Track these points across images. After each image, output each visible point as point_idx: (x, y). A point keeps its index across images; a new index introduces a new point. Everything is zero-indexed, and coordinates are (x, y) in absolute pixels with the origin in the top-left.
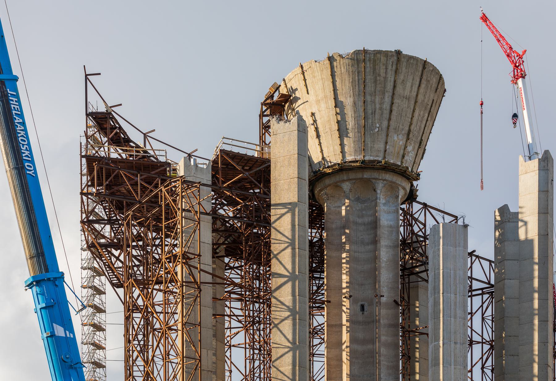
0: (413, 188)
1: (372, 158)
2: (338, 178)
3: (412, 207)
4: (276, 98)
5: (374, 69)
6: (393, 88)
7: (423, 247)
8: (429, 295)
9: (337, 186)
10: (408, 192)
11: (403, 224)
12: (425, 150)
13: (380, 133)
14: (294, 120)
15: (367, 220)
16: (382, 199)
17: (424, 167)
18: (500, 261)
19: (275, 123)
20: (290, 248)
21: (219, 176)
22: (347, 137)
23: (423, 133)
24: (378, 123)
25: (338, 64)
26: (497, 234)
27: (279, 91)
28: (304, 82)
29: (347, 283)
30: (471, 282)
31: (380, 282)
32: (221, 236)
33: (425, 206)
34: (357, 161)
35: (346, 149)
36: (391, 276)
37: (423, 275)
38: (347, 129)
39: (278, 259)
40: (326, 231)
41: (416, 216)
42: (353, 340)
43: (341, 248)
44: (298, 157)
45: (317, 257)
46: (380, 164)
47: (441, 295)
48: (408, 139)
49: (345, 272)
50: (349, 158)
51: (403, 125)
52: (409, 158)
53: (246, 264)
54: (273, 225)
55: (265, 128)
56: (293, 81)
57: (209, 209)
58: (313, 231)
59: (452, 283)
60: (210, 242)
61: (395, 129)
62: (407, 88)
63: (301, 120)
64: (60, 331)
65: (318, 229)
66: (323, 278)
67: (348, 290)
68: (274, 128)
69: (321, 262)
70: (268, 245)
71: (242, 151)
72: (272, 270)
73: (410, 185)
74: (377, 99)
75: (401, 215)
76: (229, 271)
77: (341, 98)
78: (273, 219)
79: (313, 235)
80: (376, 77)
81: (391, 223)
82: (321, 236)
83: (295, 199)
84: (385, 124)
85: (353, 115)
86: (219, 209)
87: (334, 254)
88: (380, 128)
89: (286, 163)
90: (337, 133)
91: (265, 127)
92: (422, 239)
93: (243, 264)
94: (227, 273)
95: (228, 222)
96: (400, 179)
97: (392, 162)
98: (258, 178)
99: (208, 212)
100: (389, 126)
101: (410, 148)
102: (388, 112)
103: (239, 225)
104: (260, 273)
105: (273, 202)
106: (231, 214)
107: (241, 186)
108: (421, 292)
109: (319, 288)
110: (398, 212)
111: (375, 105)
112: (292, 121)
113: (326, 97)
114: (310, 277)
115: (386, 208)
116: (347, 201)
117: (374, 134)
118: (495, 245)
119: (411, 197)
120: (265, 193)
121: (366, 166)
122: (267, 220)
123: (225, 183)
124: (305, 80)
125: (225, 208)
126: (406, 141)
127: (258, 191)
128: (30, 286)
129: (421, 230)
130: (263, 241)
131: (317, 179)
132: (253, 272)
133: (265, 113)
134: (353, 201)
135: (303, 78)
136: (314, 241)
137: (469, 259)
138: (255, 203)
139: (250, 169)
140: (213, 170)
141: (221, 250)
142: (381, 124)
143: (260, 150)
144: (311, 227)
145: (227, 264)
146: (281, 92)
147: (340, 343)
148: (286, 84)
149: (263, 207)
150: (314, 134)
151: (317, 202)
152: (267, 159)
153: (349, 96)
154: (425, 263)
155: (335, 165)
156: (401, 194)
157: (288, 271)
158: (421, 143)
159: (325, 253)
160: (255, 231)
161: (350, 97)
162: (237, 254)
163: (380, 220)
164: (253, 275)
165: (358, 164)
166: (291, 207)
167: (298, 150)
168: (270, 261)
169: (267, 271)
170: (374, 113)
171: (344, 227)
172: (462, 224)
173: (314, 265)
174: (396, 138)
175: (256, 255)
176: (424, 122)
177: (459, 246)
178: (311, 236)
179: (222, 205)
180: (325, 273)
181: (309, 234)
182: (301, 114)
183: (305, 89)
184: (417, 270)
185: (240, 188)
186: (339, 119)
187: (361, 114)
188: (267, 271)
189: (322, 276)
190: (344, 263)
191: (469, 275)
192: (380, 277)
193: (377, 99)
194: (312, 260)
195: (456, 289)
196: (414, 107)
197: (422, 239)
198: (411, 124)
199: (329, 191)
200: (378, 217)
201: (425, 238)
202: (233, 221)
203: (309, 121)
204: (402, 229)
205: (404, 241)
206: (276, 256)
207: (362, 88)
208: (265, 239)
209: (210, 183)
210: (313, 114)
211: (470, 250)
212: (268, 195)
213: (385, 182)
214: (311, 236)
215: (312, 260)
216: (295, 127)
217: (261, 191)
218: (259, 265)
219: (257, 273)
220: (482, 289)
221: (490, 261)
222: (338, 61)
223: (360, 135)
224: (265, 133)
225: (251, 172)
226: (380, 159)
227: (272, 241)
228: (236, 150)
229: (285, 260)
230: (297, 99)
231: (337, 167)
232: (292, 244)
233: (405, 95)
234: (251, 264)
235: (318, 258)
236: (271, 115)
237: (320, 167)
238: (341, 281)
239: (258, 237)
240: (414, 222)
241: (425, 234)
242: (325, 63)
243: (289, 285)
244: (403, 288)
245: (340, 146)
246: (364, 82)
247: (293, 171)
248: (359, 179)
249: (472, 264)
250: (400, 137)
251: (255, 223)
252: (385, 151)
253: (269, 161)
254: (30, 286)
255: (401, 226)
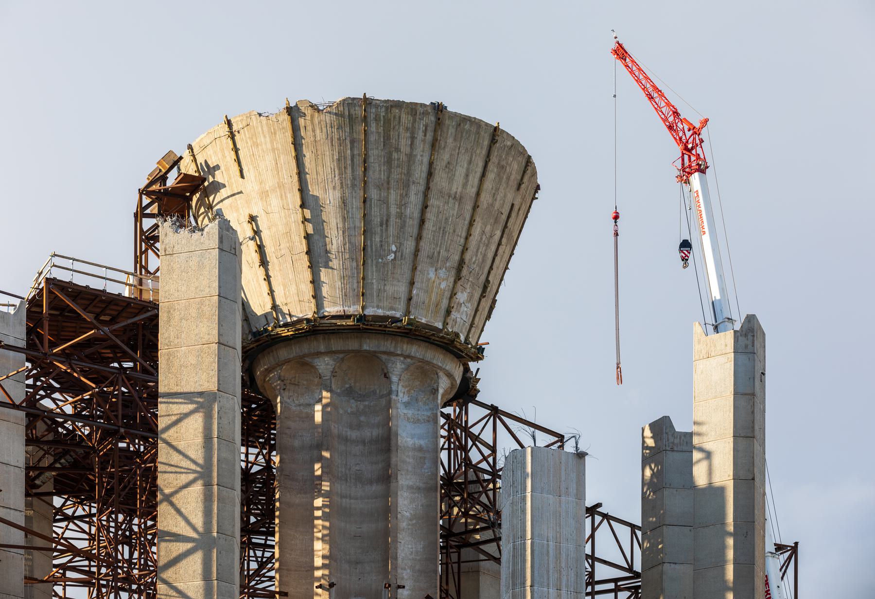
0: (469, 375)
1: (380, 312)
2: (305, 348)
3: (467, 413)
4: (172, 180)
5: (387, 138)
6: (425, 182)
7: (491, 494)
8: (503, 589)
9: (304, 364)
10: (458, 382)
11: (446, 446)
12: (494, 301)
13: (398, 262)
14: (212, 228)
15: (368, 433)
16: (401, 395)
17: (491, 335)
18: (653, 525)
19: (170, 232)
20: (200, 482)
21: (45, 332)
22: (327, 266)
23: (491, 268)
24: (394, 243)
25: (308, 123)
26: (648, 473)
27: (179, 168)
28: (233, 153)
29: (324, 557)
30: (592, 566)
31: (396, 559)
32: (47, 453)
33: (495, 412)
34: (348, 317)
35: (325, 290)
36: (420, 547)
37: (491, 548)
38: (327, 252)
39: (172, 504)
40: (279, 453)
41: (475, 430)
43: (313, 486)
44: (220, 301)
45: (259, 502)
46: (399, 324)
47: (528, 589)
48: (458, 278)
49: (320, 535)
50: (331, 309)
51: (447, 250)
53: (100, 512)
54: (164, 436)
55: (148, 240)
56: (210, 151)
57: (19, 395)
58: (251, 450)
59: (551, 566)
60: (22, 463)
61: (431, 257)
63: (226, 229)
65: (263, 447)
66: (273, 547)
67: (327, 572)
68: (167, 241)
69: (268, 514)
70: (151, 475)
71: (96, 284)
72: (160, 526)
73: (462, 368)
74: (393, 196)
75: (442, 427)
76: (63, 524)
77: (314, 190)
78: (162, 423)
79: (251, 458)
80: (390, 153)
81: (422, 442)
82: (269, 461)
83: (211, 385)
84: (409, 246)
85: (340, 225)
86: (43, 397)
87: (297, 499)
88: (399, 254)
89: (193, 312)
90: (306, 258)
91: (148, 239)
92: (487, 477)
93: (94, 511)
94: (59, 528)
95: (61, 425)
96: (441, 357)
97: (424, 321)
98: (129, 339)
99: (17, 403)
100: (417, 250)
101: (462, 297)
102: (416, 222)
103: (87, 432)
104: (131, 530)
105: (162, 389)
106: (69, 410)
107: (93, 354)
108: (485, 582)
109: (262, 565)
110: (436, 422)
111: (388, 208)
112: (206, 230)
113: (281, 186)
114: (242, 543)
115: (410, 412)
116: (325, 394)
117: (385, 265)
118: (643, 494)
119: (466, 392)
120: (144, 370)
121: (365, 326)
122: (149, 424)
123: (57, 346)
124: (236, 150)
125: (57, 395)
126: (455, 282)
127: (131, 364)
129: (485, 459)
130: (139, 467)
132: (117, 528)
133: (148, 211)
134: (339, 395)
135: (232, 146)
136: (253, 471)
137: (588, 521)
138: (123, 389)
139: (113, 321)
140: (29, 318)
141: (46, 482)
142: (400, 247)
143: (135, 283)
144: (246, 443)
145: (59, 510)
146: (183, 171)
148: (194, 156)
149: (140, 398)
150: (256, 257)
151: (261, 394)
152: (150, 302)
153: (331, 186)
154: (494, 525)
155: (300, 321)
156: (444, 384)
157: (194, 529)
158: (485, 288)
159: (277, 496)
160: (122, 445)
161: (334, 188)
162: (82, 491)
163: (397, 435)
164: (116, 534)
165: (350, 322)
166: (203, 401)
167: (220, 287)
168: (155, 507)
169: (147, 528)
170: (385, 223)
171: (319, 447)
172: (573, 450)
173: (253, 519)
174: (432, 275)
175: (123, 493)
176: (493, 248)
177: (567, 494)
178: (247, 462)
179: (52, 389)
180: (277, 535)
181: (243, 457)
182: (228, 215)
183: (237, 168)
184: (478, 537)
185: (91, 358)
186: (310, 230)
187: (358, 224)
188: (147, 528)
189: (269, 543)
190: (318, 518)
191: (588, 551)
192: (396, 549)
193: (393, 196)
194: (249, 510)
195: (559, 579)
196: (472, 216)
197: (487, 477)
198: (465, 249)
199: (285, 372)
200: (394, 429)
201: (495, 474)
202: (73, 423)
203: (244, 231)
204: (444, 455)
205: (448, 479)
206: (168, 498)
208: (145, 462)
209: (22, 344)
210: (252, 219)
211: (589, 503)
212: (152, 375)
213: (409, 360)
214: (247, 462)
215: (249, 510)
216: (214, 242)
217: (135, 365)
218: (130, 514)
219: (125, 530)
220: (615, 581)
221: (633, 527)
222: (308, 118)
223: (354, 264)
224: (146, 250)
225: (115, 327)
226: (398, 315)
227: (161, 468)
228: (81, 281)
229: (187, 505)
230: (217, 187)
231: (304, 325)
232: (204, 475)
233: (453, 192)
234: (112, 512)
235: (262, 505)
236: (160, 214)
237: (268, 324)
238: (311, 553)
239: (127, 458)
240: (470, 443)
241: (493, 467)
242: (281, 119)
243: (198, 557)
244: (446, 571)
245: (311, 285)
246: (365, 162)
247: (209, 330)
248: (353, 351)
249: (594, 529)
250: (442, 273)
251: (122, 430)
252: (410, 299)
253: (154, 306)
255: (442, 449)
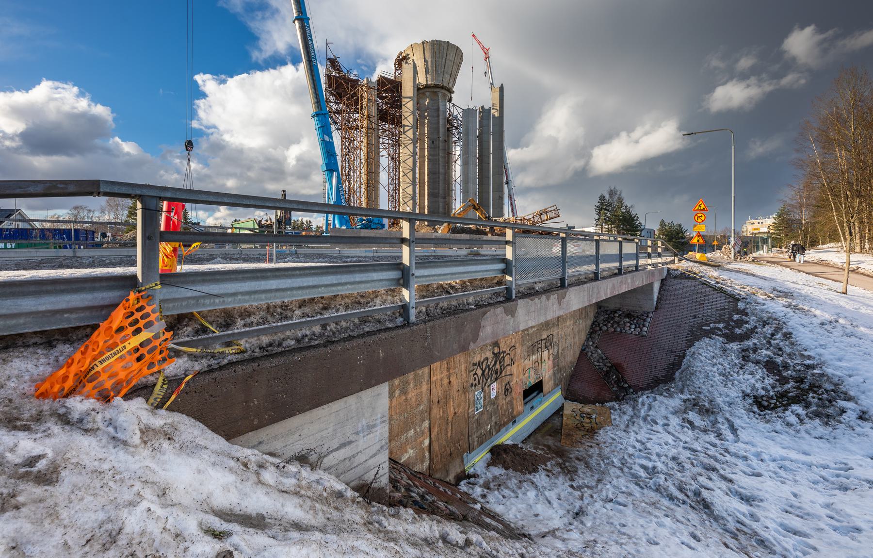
6: (444, 56)
9: (424, 94)
42: (430, 155)
52: (451, 84)
62: (451, 57)
64: (327, 138)
121: (436, 86)
128: (313, 117)
131: (420, 90)
147: (424, 156)
207: (434, 54)
254: (313, 117)
